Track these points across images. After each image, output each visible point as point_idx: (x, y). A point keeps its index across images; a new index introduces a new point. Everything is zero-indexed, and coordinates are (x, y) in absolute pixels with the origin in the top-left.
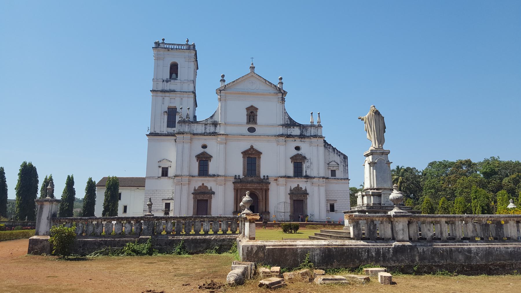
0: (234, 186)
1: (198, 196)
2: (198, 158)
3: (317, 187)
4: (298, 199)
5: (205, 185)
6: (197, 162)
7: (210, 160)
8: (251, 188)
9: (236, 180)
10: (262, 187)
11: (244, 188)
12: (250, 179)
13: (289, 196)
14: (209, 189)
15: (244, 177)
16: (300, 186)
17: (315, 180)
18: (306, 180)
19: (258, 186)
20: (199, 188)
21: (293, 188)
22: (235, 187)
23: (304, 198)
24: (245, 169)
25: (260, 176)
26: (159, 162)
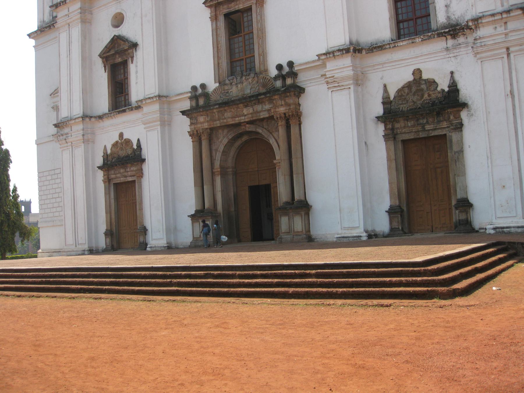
0: (192, 124)
1: (113, 172)
2: (104, 60)
3: (500, 62)
4: (422, 135)
5: (125, 137)
6: (105, 72)
7: (132, 57)
8: (237, 120)
9: (194, 104)
10: (272, 111)
11: (218, 124)
12: (235, 91)
13: (381, 127)
14: (135, 147)
15: (217, 85)
16: (425, 76)
17: (482, 32)
18: (451, 42)
19: (259, 107)
20: (113, 149)
21: (399, 91)
22: (193, 127)
23: (445, 124)
24: (219, 58)
25: (266, 71)
26: (50, 95)
